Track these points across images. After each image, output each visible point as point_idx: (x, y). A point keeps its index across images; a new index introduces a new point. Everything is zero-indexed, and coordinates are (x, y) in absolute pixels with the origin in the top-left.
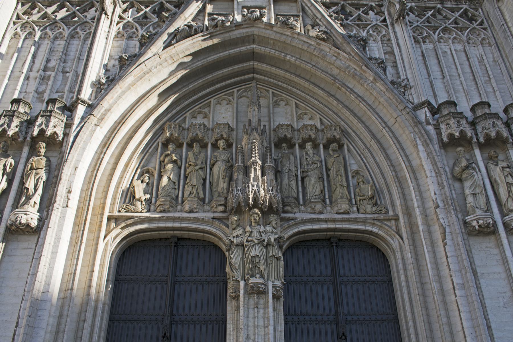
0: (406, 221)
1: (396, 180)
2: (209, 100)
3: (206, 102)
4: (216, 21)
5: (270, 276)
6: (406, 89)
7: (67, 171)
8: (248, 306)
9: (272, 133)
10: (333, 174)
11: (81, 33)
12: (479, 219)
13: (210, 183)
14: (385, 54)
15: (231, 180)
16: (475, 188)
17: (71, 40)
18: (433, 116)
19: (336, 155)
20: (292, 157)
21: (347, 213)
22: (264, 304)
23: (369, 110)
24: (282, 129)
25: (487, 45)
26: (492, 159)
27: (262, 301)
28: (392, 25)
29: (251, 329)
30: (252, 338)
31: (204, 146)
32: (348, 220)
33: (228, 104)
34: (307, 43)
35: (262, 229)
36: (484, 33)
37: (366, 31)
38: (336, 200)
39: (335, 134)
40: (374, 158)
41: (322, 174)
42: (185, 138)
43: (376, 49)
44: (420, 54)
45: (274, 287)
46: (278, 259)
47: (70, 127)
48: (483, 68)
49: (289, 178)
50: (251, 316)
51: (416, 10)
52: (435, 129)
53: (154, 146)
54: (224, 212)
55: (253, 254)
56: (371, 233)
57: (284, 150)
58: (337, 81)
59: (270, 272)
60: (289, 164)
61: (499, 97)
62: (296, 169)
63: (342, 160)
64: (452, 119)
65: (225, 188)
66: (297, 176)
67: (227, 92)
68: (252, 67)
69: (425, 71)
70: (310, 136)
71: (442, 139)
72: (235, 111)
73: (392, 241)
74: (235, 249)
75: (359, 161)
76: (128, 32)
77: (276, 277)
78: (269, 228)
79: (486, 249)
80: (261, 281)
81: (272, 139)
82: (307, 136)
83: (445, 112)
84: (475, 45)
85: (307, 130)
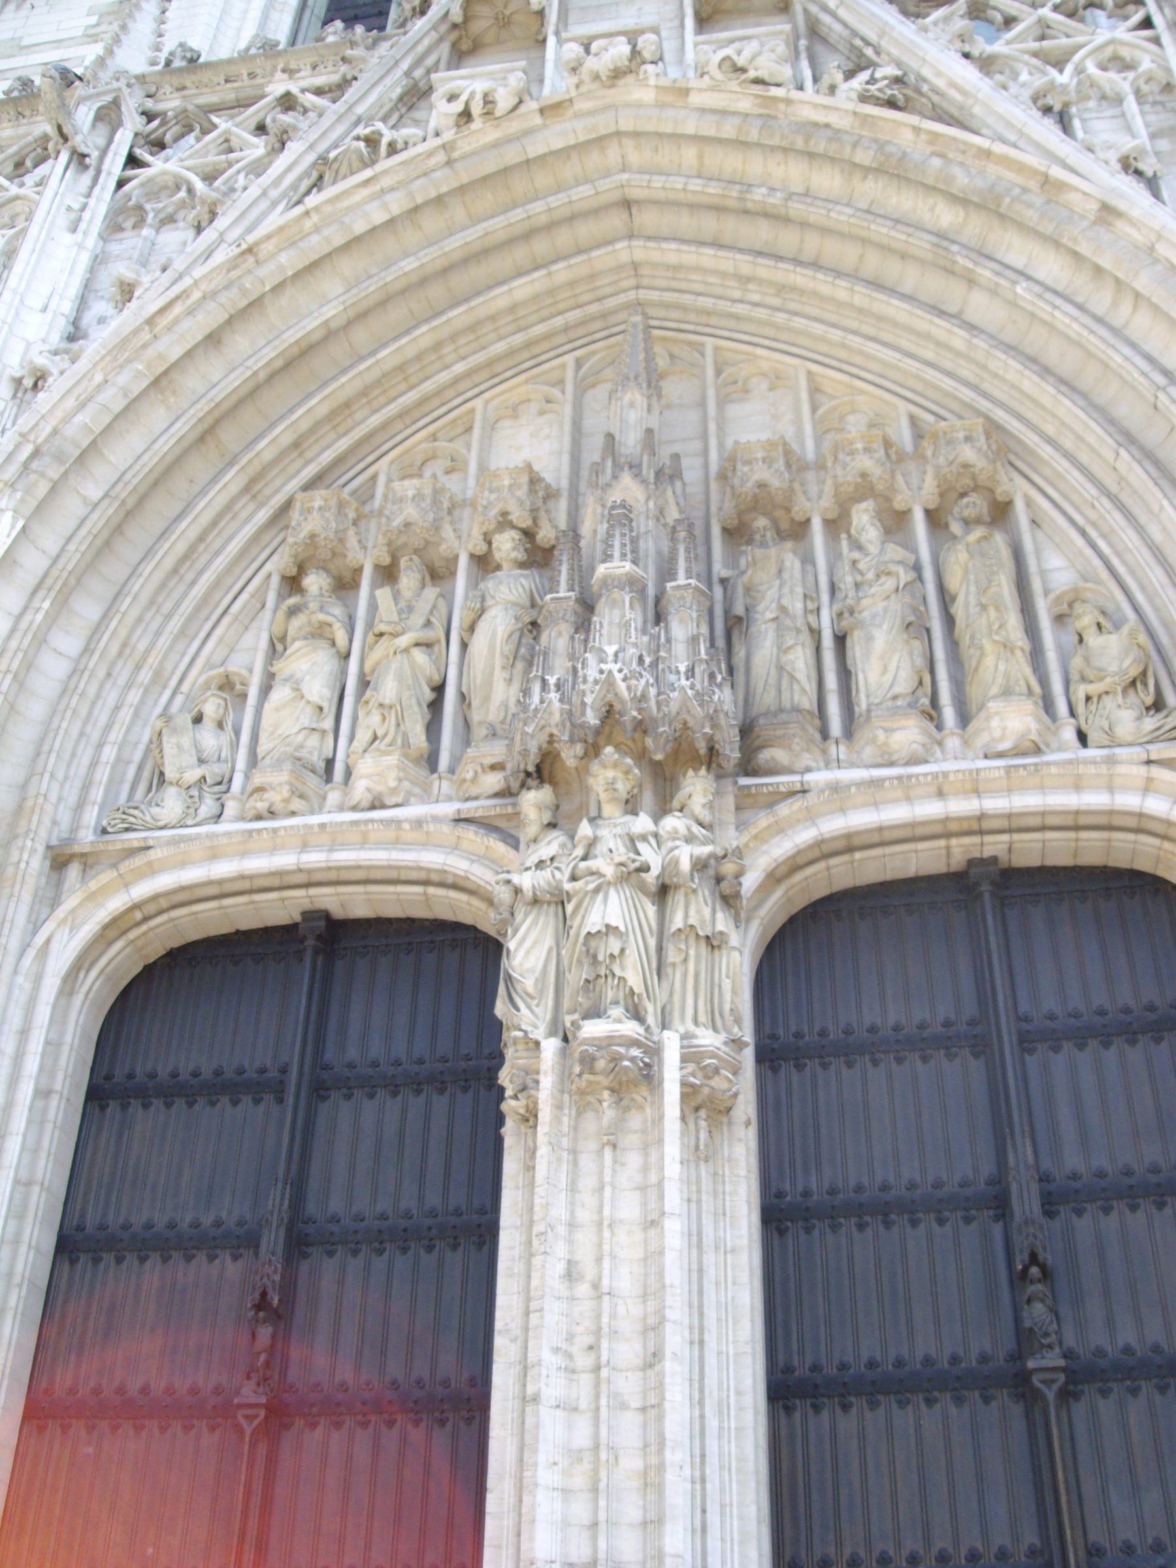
2: (469, 405)
4: (464, 98)
5: (676, 1014)
8: (575, 1140)
9: (714, 486)
10: (967, 605)
13: (462, 697)
14: (1153, 136)
22: (644, 1131)
27: (635, 1121)
29: (585, 1239)
30: (590, 1272)
33: (541, 413)
34: (827, 126)
40: (1140, 529)
45: (689, 1056)
49: (780, 636)
50: (587, 1183)
55: (594, 920)
59: (677, 998)
60: (781, 587)
62: (811, 605)
66: (816, 633)
74: (526, 915)
75: (1081, 553)
77: (702, 1018)
80: (631, 1028)
81: (714, 509)
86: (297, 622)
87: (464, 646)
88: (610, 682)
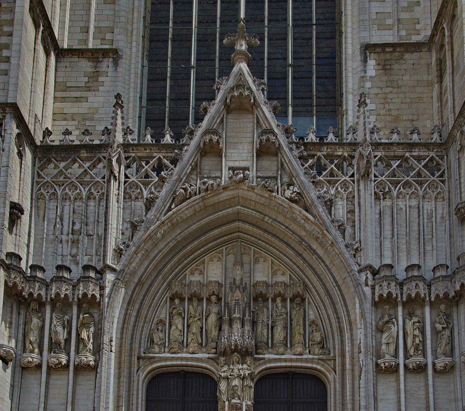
0: (340, 361)
1: (338, 330)
3: (201, 260)
6: (357, 251)
7: (107, 325)
11: (95, 193)
12: (386, 362)
15: (220, 329)
16: (390, 338)
17: (88, 201)
18: (374, 276)
19: (298, 309)
20: (265, 310)
21: (301, 354)
23: (325, 271)
24: (259, 286)
25: (441, 200)
26: (411, 315)
28: (358, 181)
31: (200, 300)
32: (301, 360)
35: (240, 366)
36: (441, 185)
37: (335, 188)
38: (294, 345)
39: (299, 290)
41: (286, 324)
42: (187, 293)
43: (341, 207)
44: (378, 212)
46: (250, 387)
47: (104, 289)
48: (430, 225)
51: (385, 161)
52: (372, 289)
53: (164, 300)
54: (215, 353)
55: (233, 384)
56: (316, 369)
57: (260, 304)
58: (303, 243)
61: (434, 256)
63: (303, 313)
64: (385, 282)
65: (216, 335)
67: (217, 250)
68: (237, 226)
69: (379, 230)
70: (280, 292)
71: (374, 299)
72: (224, 268)
73: (329, 375)
76: (135, 193)
78: (245, 366)
79: (389, 383)
80: (239, 401)
82: (278, 292)
83: (382, 274)
84: (430, 200)
85: (278, 286)
86: (175, 311)
87: (206, 320)
88: (236, 341)
